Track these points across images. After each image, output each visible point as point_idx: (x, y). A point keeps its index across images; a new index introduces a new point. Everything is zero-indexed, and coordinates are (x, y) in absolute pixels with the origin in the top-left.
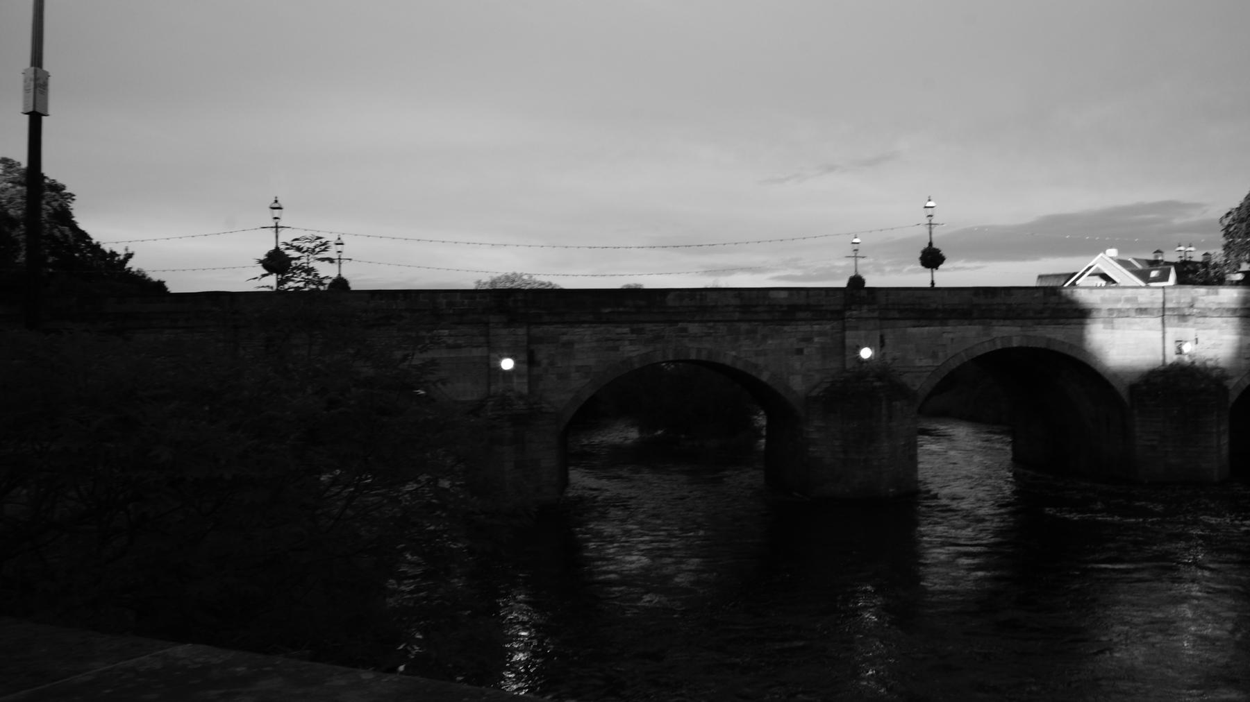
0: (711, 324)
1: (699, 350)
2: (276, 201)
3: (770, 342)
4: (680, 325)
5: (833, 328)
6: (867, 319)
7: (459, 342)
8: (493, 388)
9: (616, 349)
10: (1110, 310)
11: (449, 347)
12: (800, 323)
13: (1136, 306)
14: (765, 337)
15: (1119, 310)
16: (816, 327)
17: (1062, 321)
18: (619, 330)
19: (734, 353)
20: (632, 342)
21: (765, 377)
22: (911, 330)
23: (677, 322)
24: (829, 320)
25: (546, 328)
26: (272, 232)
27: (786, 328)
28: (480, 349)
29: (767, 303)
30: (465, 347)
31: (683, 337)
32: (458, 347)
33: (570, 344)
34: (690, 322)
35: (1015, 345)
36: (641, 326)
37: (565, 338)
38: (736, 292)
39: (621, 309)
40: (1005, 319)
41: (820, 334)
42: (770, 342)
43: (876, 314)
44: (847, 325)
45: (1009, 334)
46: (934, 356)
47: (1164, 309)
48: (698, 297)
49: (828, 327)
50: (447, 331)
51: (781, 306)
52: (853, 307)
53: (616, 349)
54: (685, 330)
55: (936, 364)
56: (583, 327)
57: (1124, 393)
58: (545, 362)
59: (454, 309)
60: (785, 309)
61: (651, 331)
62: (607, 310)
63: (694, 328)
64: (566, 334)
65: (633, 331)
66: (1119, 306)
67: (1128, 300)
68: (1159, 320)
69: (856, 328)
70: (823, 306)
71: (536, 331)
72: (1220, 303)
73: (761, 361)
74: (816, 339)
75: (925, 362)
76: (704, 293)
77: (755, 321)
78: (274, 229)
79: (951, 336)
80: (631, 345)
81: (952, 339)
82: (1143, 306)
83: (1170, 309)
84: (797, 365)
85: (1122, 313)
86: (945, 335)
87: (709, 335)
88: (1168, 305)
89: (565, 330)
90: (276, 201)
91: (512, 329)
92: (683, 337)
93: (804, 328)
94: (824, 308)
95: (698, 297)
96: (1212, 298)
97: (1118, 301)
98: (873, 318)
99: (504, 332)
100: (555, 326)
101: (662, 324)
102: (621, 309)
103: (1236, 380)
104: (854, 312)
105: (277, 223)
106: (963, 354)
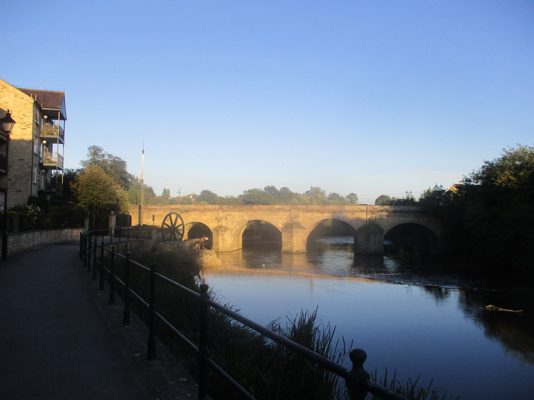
1: (260, 218)
9: (243, 217)
11: (211, 216)
15: (356, 211)
16: (285, 214)
19: (267, 218)
21: (273, 224)
22: (305, 214)
27: (278, 213)
37: (233, 215)
40: (328, 212)
41: (286, 215)
42: (275, 216)
47: (367, 211)
49: (287, 214)
53: (243, 217)
57: (356, 229)
58: (229, 220)
63: (259, 213)
64: (233, 214)
66: (356, 210)
67: (358, 208)
68: (366, 213)
71: (227, 213)
73: (273, 220)
75: (309, 221)
81: (315, 217)
84: (280, 221)
88: (368, 210)
97: (356, 209)
99: (221, 213)
103: (386, 228)
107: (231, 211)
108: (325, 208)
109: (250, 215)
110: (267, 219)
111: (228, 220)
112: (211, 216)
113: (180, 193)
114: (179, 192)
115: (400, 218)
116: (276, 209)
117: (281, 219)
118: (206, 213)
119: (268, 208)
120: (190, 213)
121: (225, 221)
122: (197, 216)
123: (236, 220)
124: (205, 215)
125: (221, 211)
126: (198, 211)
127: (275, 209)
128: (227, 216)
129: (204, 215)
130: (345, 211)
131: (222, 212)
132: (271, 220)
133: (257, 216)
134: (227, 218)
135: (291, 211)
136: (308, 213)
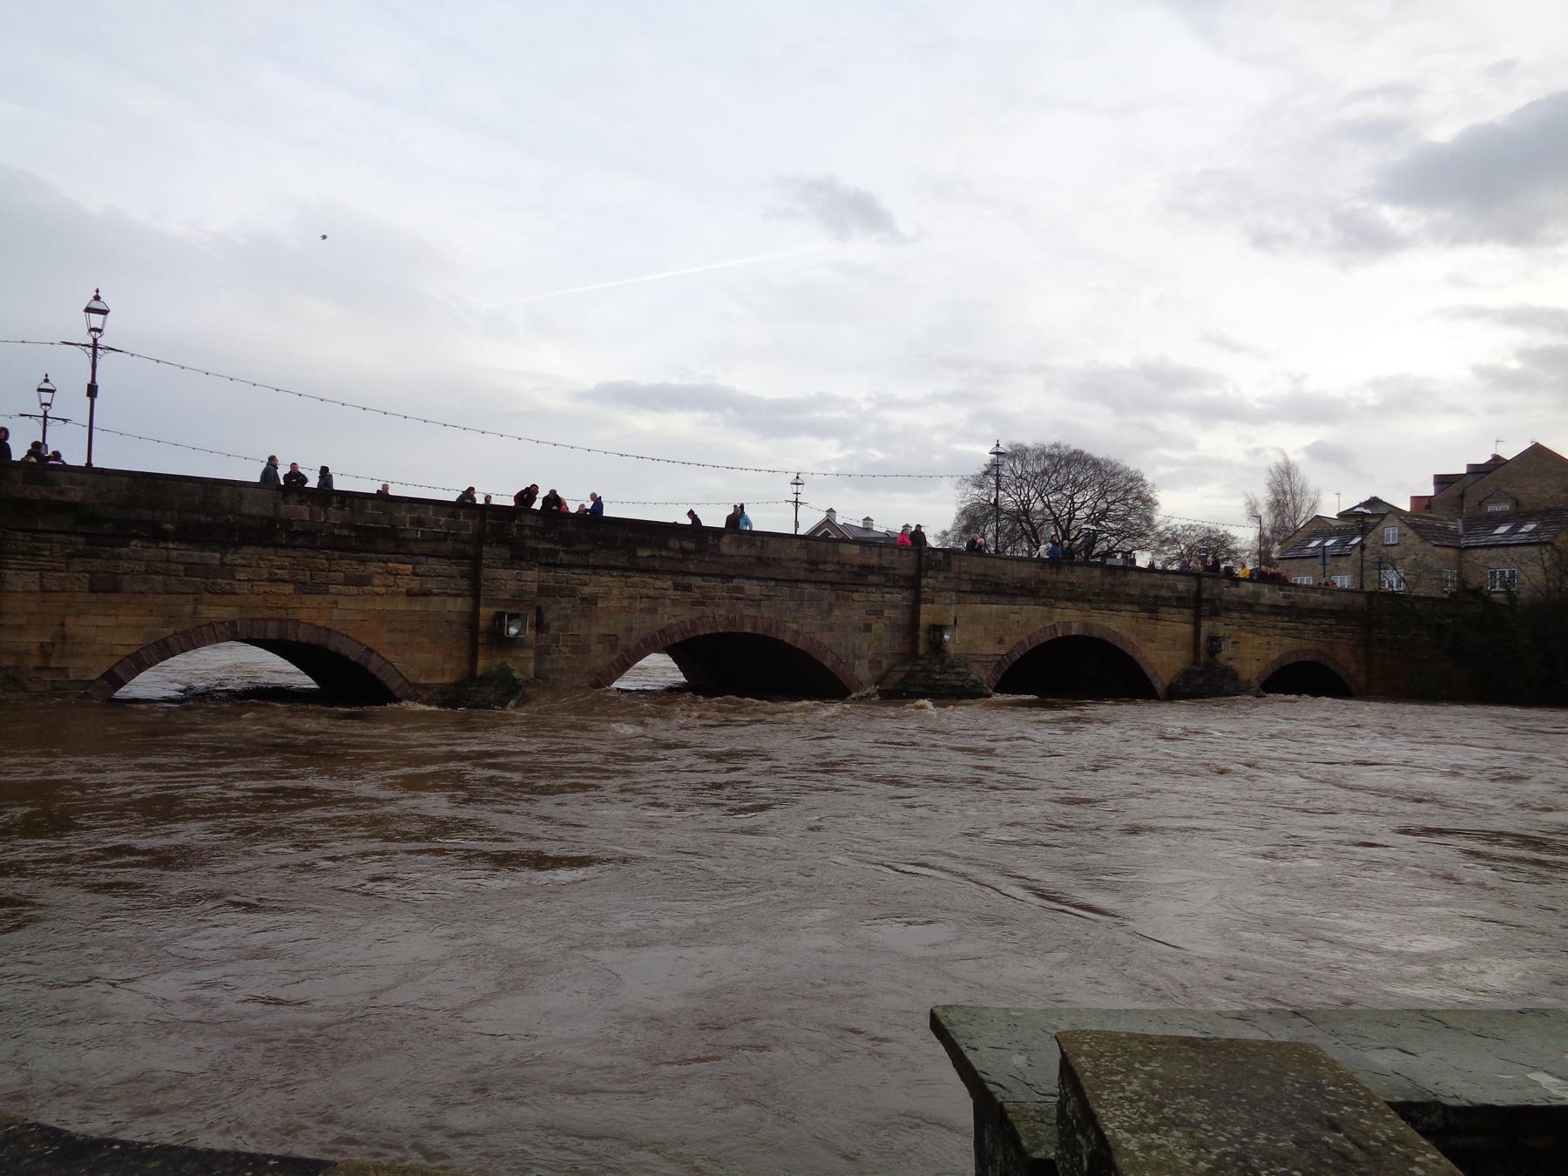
0: (773, 583)
2: (97, 298)
3: (837, 612)
4: (736, 582)
5: (905, 599)
6: (943, 590)
7: (428, 586)
8: (482, 664)
10: (1156, 597)
11: (410, 594)
12: (870, 589)
13: (1176, 594)
14: (831, 608)
15: (1164, 598)
17: (1116, 606)
18: (659, 584)
19: (795, 626)
20: (675, 602)
23: (733, 577)
24: (901, 588)
25: (563, 573)
26: (84, 358)
27: (855, 596)
28: (460, 599)
29: (836, 559)
30: (438, 594)
31: (737, 599)
32: (427, 594)
33: (591, 601)
34: (748, 578)
35: (1073, 633)
36: (686, 580)
37: (587, 590)
38: (803, 542)
39: (664, 553)
41: (894, 606)
43: (952, 585)
44: (923, 596)
45: (1070, 619)
46: (1001, 641)
48: (759, 544)
50: (410, 567)
51: (852, 566)
52: (930, 573)
53: (654, 611)
54: (740, 589)
55: (1003, 652)
56: (612, 576)
58: (555, 626)
59: (422, 531)
60: (856, 569)
61: (700, 588)
62: (643, 553)
63: (751, 588)
64: (586, 585)
65: (676, 587)
66: (1164, 592)
68: (1192, 612)
69: (933, 602)
70: (895, 569)
72: (1240, 597)
73: (825, 638)
74: (886, 613)
76: (765, 538)
77: (823, 583)
78: (90, 350)
79: (1017, 617)
80: (675, 605)
82: (1182, 595)
83: (1206, 600)
85: (1166, 602)
86: (1012, 616)
87: (769, 597)
89: (586, 578)
90: (97, 298)
91: (515, 572)
92: (737, 599)
93: (876, 597)
94: (897, 572)
95: (759, 544)
96: (1233, 589)
97: (1161, 587)
98: (948, 590)
99: (502, 574)
100: (571, 571)
101: (714, 580)
102: (664, 553)
104: (930, 580)
105: (95, 340)
106: (1027, 641)
107: (578, 560)
108: (1061, 577)
109: (697, 594)
110: (797, 633)
111: (548, 631)
112: (410, 594)
113: (104, 359)
114: (95, 346)
115: (1288, 641)
116: (848, 567)
117: (868, 628)
118: (372, 567)
119: (803, 555)
120: (213, 557)
121: (530, 634)
122: (288, 589)
123: (603, 631)
124: (362, 581)
125: (505, 552)
126: (301, 541)
127: (844, 564)
128: (542, 601)
129: (346, 583)
130: (1128, 595)
131: (507, 565)
132: (818, 637)
133: (741, 605)
134: (548, 616)
135: (924, 581)
136: (994, 598)
